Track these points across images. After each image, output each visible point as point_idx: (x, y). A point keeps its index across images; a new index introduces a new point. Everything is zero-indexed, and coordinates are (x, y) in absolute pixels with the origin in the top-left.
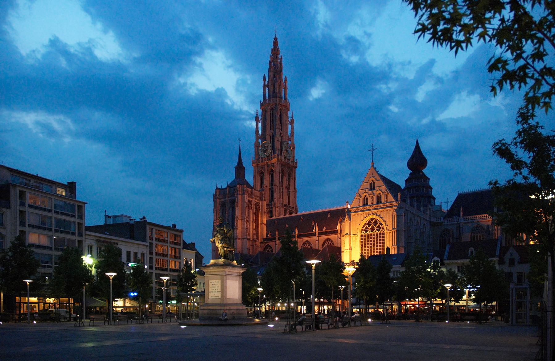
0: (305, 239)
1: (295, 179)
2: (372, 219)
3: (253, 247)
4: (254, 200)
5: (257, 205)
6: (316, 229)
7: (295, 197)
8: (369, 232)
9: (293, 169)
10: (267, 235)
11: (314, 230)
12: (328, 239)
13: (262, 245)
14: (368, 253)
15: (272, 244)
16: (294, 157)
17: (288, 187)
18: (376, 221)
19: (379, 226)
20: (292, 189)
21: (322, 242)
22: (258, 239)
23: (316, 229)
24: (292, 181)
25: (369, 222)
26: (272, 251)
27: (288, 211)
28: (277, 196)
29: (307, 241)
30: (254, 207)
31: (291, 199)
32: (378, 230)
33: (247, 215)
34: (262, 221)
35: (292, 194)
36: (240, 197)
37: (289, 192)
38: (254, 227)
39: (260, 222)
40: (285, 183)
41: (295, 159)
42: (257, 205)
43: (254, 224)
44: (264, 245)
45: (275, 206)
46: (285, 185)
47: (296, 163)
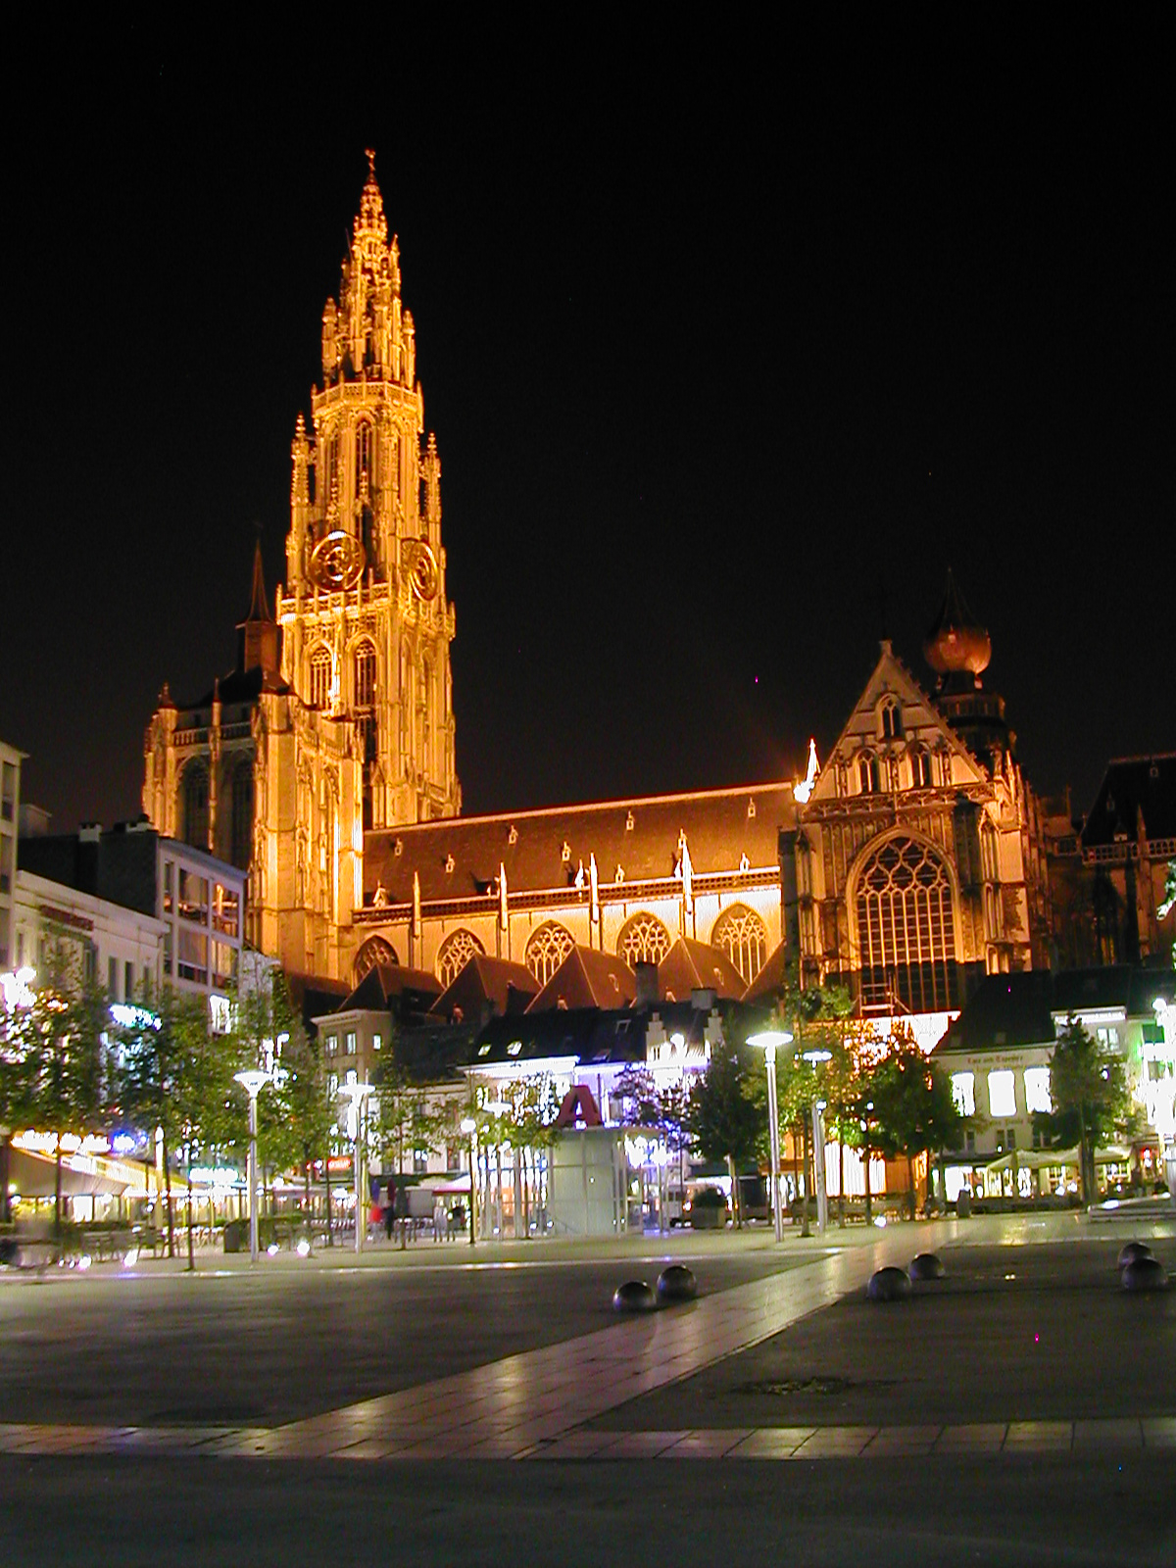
0: (542, 915)
2: (900, 841)
3: (320, 947)
6: (586, 880)
8: (891, 889)
10: (368, 899)
11: (579, 881)
12: (648, 918)
13: (348, 937)
15: (394, 932)
18: (913, 850)
19: (926, 869)
21: (618, 928)
22: (331, 912)
23: (586, 880)
25: (888, 853)
26: (396, 961)
28: (387, 741)
29: (552, 925)
32: (927, 882)
34: (347, 839)
36: (273, 740)
38: (323, 866)
43: (323, 851)
44: (356, 940)
45: (382, 779)
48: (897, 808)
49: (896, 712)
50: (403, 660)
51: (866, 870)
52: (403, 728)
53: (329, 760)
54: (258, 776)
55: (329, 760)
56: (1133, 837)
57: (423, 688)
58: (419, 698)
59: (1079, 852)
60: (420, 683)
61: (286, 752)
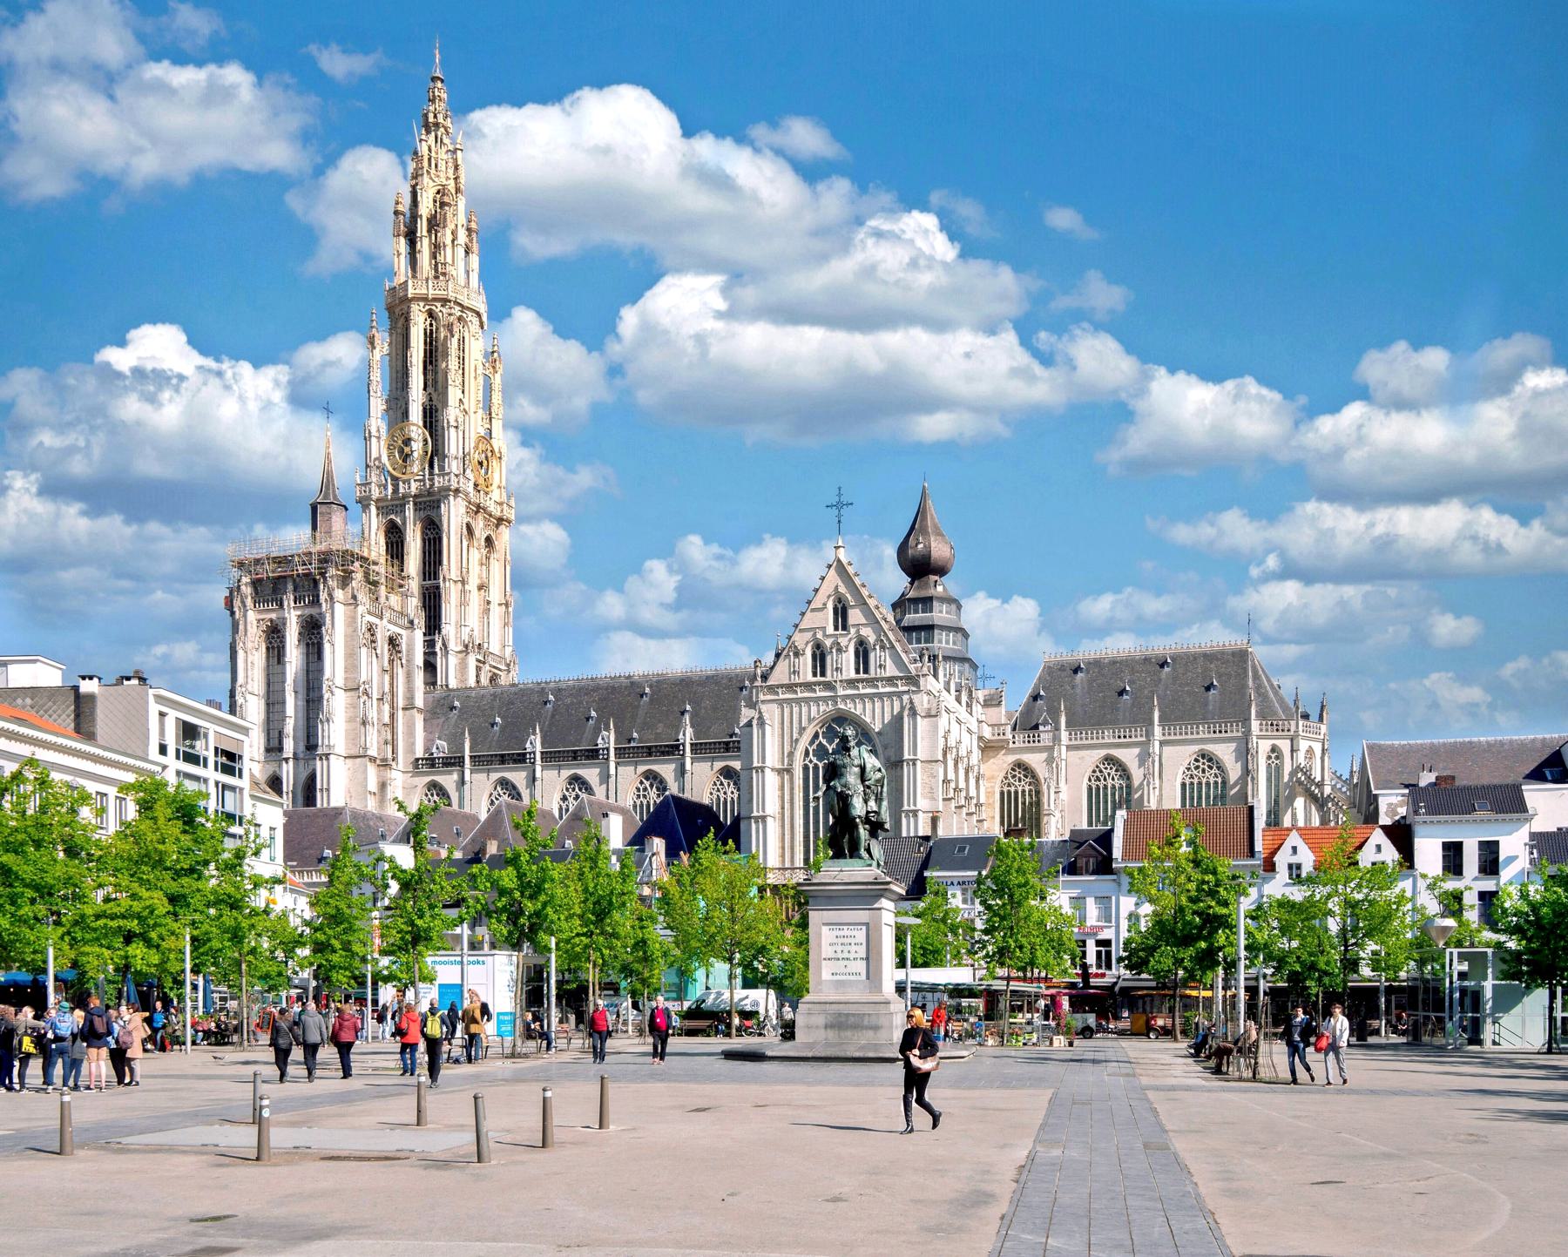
4: (385, 628)
5: (393, 642)
37: (489, 603)
42: (393, 642)
48: (841, 692)
50: (465, 543)
51: (812, 743)
52: (463, 603)
54: (326, 638)
61: (351, 621)
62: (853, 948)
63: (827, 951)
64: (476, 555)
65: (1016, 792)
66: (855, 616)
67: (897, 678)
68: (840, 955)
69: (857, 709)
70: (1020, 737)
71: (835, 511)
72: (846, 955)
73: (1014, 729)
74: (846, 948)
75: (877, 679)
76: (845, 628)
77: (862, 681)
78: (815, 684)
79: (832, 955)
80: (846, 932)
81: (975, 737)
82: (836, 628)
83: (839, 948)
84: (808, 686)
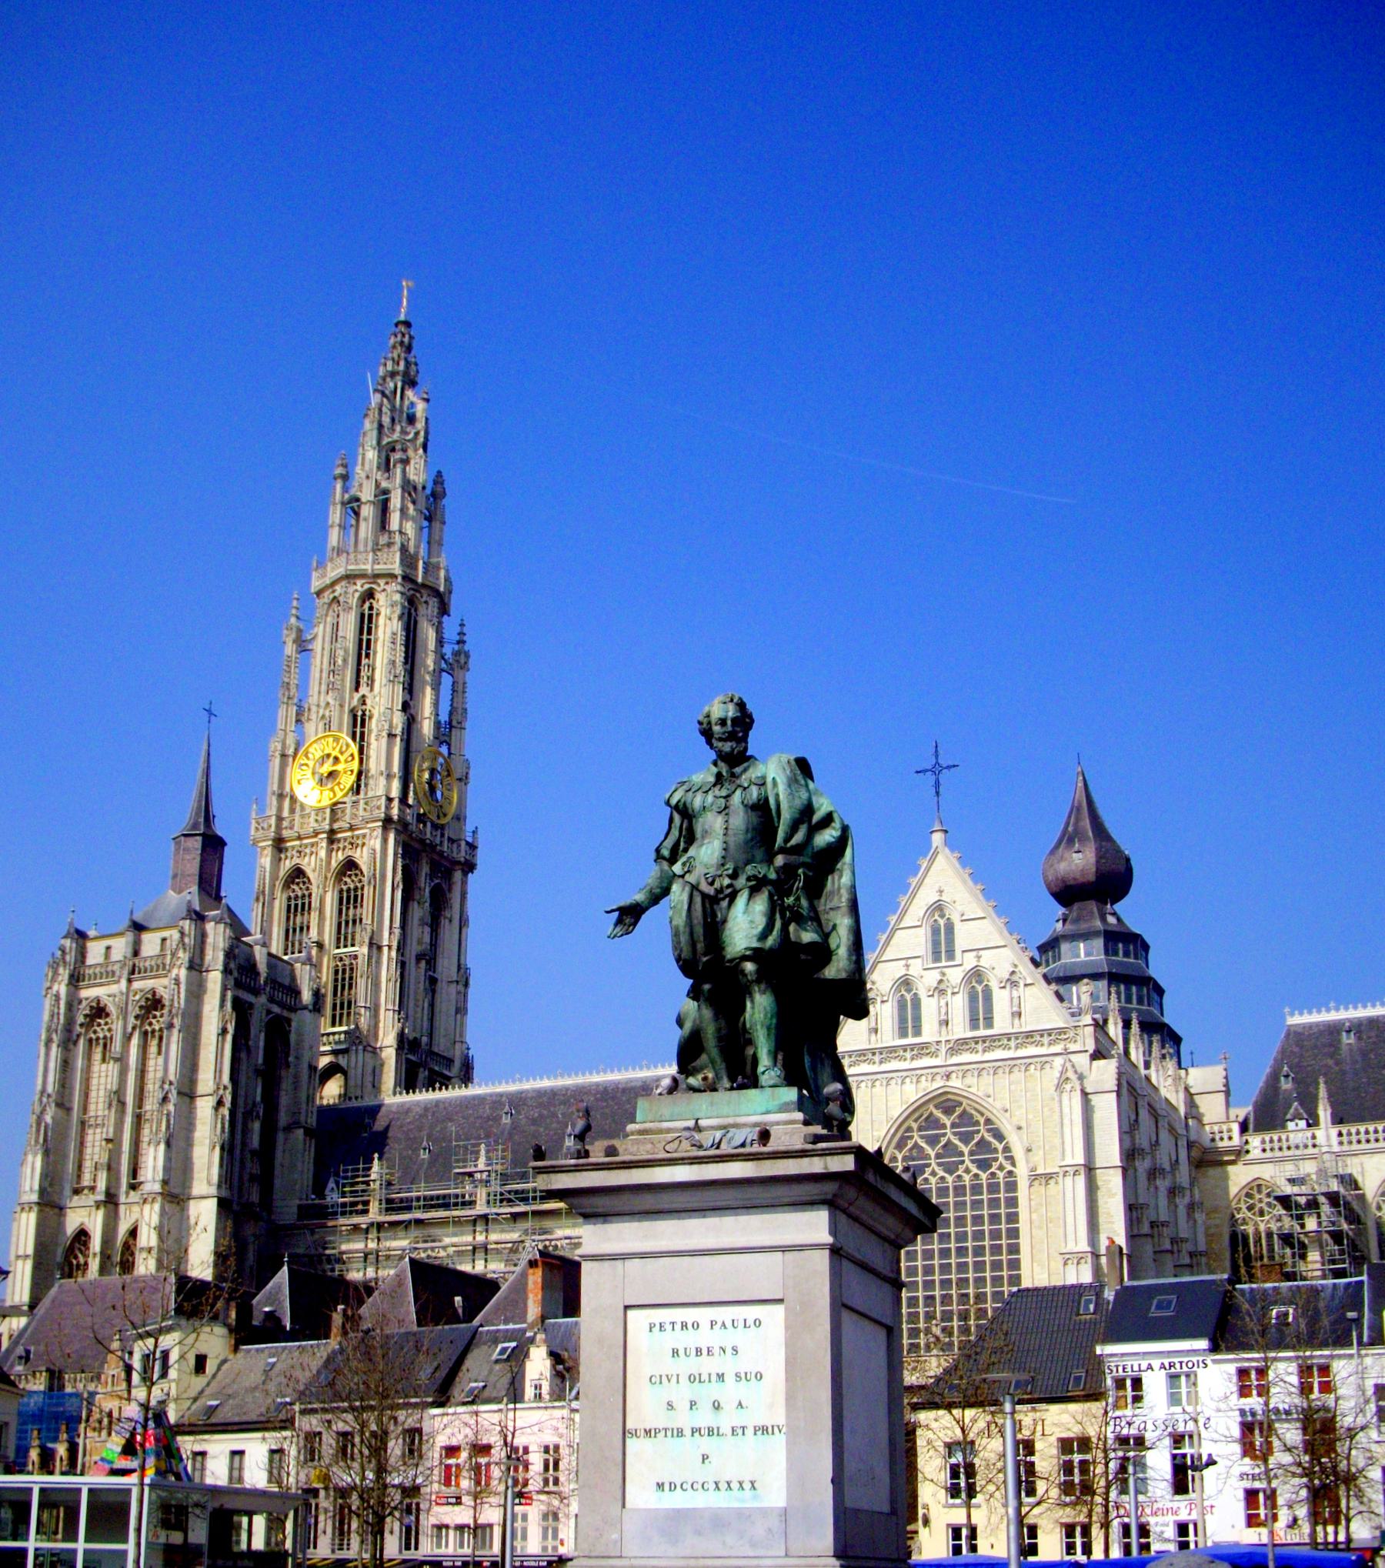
1: (463, 922)
7: (461, 1010)
9: (458, 875)
14: (997, 1281)
16: (459, 818)
17: (429, 957)
20: (446, 967)
24: (449, 933)
27: (423, 1074)
30: (259, 1040)
31: (444, 1022)
33: (226, 1078)
35: (447, 994)
37: (433, 981)
38: (255, 1141)
39: (283, 1119)
40: (420, 935)
41: (469, 827)
43: (256, 1126)
46: (413, 948)
47: (472, 847)
49: (950, 928)
53: (276, 1009)
55: (276, 1009)
56: (1313, 1122)
57: (427, 929)
58: (420, 942)
59: (1236, 1140)
60: (423, 923)
62: (729, 1392)
63: (646, 1406)
64: (418, 912)
65: (1257, 1233)
66: (964, 937)
67: (1041, 1033)
68: (684, 1419)
69: (974, 1088)
70: (1255, 1141)
71: (930, 778)
72: (704, 1417)
73: (1244, 1128)
74: (714, 1391)
75: (1008, 1036)
76: (951, 955)
77: (984, 1039)
78: (904, 1048)
79: (657, 1418)
80: (705, 1337)
81: (1182, 1143)
82: (936, 956)
83: (682, 1393)
84: (891, 1052)
